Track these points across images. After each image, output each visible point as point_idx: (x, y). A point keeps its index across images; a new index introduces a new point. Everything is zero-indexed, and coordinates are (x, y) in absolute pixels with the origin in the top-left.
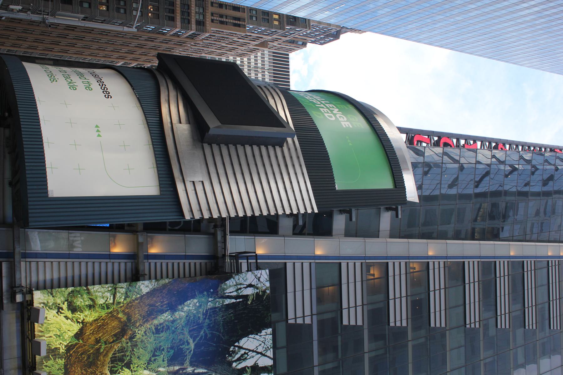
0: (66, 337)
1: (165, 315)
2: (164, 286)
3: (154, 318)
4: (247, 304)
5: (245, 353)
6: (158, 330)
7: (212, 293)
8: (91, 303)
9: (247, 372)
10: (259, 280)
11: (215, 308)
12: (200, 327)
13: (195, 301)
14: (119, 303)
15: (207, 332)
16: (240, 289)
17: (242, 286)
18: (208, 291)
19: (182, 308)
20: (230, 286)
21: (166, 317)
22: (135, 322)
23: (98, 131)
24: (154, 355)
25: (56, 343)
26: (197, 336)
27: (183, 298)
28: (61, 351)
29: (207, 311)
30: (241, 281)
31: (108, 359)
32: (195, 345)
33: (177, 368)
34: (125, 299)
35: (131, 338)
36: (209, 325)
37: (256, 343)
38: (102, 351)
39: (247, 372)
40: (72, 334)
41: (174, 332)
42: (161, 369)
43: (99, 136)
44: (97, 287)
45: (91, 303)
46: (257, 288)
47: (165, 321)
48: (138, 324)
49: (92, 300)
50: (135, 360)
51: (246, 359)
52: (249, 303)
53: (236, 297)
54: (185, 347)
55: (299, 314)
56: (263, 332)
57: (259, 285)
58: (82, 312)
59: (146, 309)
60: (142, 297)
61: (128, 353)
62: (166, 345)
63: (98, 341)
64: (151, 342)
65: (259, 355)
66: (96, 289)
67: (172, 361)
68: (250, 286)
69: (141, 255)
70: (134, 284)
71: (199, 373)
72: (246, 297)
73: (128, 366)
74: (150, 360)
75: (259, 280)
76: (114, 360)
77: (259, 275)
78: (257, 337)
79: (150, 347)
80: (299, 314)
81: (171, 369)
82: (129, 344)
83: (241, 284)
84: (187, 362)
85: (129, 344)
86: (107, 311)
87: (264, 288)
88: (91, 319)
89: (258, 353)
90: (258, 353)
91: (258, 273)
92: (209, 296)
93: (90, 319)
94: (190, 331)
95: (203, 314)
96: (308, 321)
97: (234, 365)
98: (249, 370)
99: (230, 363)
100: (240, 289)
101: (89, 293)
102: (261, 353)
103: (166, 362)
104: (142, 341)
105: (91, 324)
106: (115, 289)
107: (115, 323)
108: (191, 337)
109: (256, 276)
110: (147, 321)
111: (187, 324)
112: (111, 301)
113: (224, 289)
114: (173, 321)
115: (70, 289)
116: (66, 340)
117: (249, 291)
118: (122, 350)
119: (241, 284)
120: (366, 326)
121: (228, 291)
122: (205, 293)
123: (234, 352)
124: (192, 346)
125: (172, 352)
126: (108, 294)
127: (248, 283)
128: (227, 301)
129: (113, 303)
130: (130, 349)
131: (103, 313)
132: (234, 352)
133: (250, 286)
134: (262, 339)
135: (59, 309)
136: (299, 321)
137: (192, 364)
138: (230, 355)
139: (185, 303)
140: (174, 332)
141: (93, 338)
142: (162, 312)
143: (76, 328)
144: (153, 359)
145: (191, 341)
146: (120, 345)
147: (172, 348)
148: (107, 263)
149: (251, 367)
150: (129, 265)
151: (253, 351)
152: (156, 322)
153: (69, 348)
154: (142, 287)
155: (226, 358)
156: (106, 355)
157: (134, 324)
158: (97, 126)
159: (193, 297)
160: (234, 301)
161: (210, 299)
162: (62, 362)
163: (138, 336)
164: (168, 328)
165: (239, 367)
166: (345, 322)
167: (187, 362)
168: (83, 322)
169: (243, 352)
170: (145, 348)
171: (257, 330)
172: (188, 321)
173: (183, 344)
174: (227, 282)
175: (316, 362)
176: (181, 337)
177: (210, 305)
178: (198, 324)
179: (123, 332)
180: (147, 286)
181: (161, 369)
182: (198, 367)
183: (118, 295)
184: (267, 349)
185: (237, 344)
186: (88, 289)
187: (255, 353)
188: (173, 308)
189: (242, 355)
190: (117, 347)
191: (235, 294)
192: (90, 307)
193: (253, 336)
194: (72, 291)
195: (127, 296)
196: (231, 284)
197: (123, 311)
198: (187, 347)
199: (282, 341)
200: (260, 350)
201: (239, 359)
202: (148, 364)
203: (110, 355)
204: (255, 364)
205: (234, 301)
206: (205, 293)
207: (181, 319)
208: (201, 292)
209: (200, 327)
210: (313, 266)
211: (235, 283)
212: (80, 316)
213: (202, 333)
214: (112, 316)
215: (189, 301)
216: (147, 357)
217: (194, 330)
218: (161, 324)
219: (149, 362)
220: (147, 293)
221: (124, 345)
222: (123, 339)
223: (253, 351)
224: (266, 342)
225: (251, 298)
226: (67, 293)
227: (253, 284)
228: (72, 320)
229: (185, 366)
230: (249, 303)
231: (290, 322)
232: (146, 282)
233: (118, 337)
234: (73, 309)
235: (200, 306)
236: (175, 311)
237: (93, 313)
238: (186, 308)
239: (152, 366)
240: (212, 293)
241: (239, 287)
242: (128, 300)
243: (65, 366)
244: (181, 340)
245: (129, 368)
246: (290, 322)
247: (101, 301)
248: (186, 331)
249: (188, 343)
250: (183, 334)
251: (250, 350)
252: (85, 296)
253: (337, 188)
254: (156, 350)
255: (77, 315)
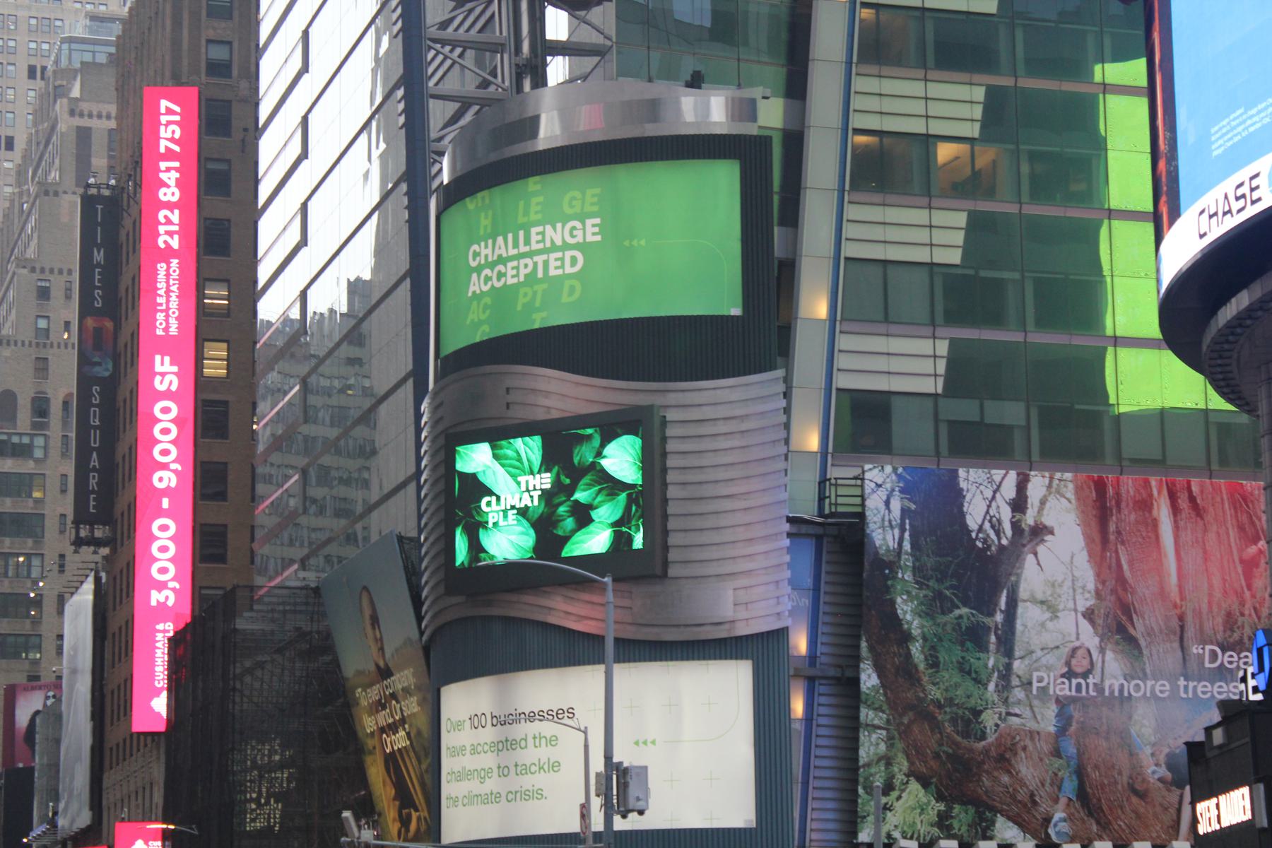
0: (924, 800)
1: (913, 650)
2: (871, 648)
3: (917, 670)
4: (914, 512)
5: (990, 521)
6: (934, 664)
7: (891, 571)
8: (883, 762)
9: (1019, 521)
10: (880, 486)
11: (914, 567)
12: (939, 595)
13: (899, 600)
14: (888, 721)
15: (948, 584)
16: (890, 521)
17: (887, 518)
18: (887, 578)
19: (908, 622)
20: (884, 539)
21: (916, 650)
22: (919, 699)
23: (645, 743)
24: (969, 673)
25: (932, 815)
26: (952, 601)
27: (893, 620)
28: (942, 808)
29: (917, 583)
30: (877, 519)
31: (965, 742)
32: (965, 605)
33: (993, 638)
34: (883, 712)
35: (939, 706)
36: (937, 580)
37: (979, 497)
38: (950, 751)
39: (1019, 521)
40: (922, 792)
41: (940, 640)
42: (991, 663)
43: (653, 742)
44: (862, 753)
45: (883, 762)
46: (893, 490)
47: (922, 652)
48: (922, 695)
49: (879, 760)
50: (972, 702)
51: (999, 521)
52: (913, 507)
53: (903, 530)
54: (965, 623)
55: (927, 366)
56: (963, 485)
57: (888, 486)
58: (893, 777)
59: (901, 680)
60: (883, 685)
61: (960, 712)
62: (958, 652)
63: (937, 756)
64: (949, 676)
65: (998, 495)
66: (864, 754)
67: (982, 647)
68: (887, 503)
69: (812, 672)
70: (863, 697)
71: (1007, 603)
72: (905, 512)
73: (977, 713)
74: (975, 680)
75: (880, 486)
76: (966, 734)
77: (873, 485)
78: (968, 497)
79: (957, 678)
80: (927, 366)
81: (992, 647)
82: (948, 710)
83: (883, 520)
84: (987, 620)
85: (948, 710)
86: (897, 741)
87: (894, 477)
88: (906, 763)
89: (994, 497)
90: (994, 497)
91: (869, 486)
92: (895, 578)
93: (905, 765)
94: (943, 613)
95: (920, 589)
96: (943, 348)
97: (1004, 542)
98: (1018, 516)
99: (1001, 548)
100: (890, 521)
101: (868, 765)
102: (995, 492)
103: (982, 655)
104: (946, 690)
105: (912, 763)
106: (867, 725)
107: (916, 729)
108: (951, 612)
109: (873, 491)
110: (919, 680)
111: (933, 618)
112: (884, 732)
113: (888, 550)
114: (925, 639)
115: (861, 791)
116: (929, 802)
117: (896, 505)
118: (954, 721)
119: (883, 520)
120: (970, 204)
121: (891, 544)
122: (889, 583)
123: (985, 541)
124: (964, 611)
125: (969, 644)
126: (874, 736)
127: (882, 506)
128: (907, 546)
129: (887, 729)
130: (955, 709)
131: (899, 745)
132: (985, 541)
133: (887, 503)
134: (974, 488)
135: (887, 808)
136: (941, 367)
137: (991, 614)
138: (989, 547)
139: (901, 617)
140: (940, 640)
141: (932, 763)
142: (909, 655)
143: (914, 786)
144: (974, 675)
145: (957, 612)
146: (946, 724)
147: (962, 644)
148: (818, 726)
149: (1013, 511)
150: (823, 689)
151: (989, 506)
152: (922, 667)
153: (940, 798)
154: (869, 684)
155: (992, 556)
156: (957, 744)
157: (920, 700)
158: (637, 743)
159: (893, 602)
160: (907, 535)
161: (900, 575)
162: (957, 809)
163: (938, 696)
164: (933, 648)
165: (1009, 532)
166: (955, 257)
167: (987, 620)
168: (907, 776)
169: (987, 525)
170: (957, 686)
171: (958, 495)
172: (927, 614)
173: (959, 625)
174: (878, 543)
175: (1017, 337)
176: (949, 628)
177: (908, 576)
178: (934, 599)
179: (930, 718)
180: (869, 676)
181: (991, 663)
182: (996, 604)
183: (876, 722)
184: (991, 481)
185: (974, 535)
186: (864, 766)
187: (994, 504)
188: (905, 638)
189: (993, 527)
190: (949, 729)
191: (897, 532)
192: (889, 764)
193: (966, 505)
194: (865, 788)
195: (880, 709)
196: (880, 537)
197: (901, 715)
198: (965, 620)
199: (874, 69)
200: (989, 494)
201: (998, 533)
202: (979, 682)
203: (959, 739)
204: (1009, 504)
205: (907, 535)
206: (889, 583)
207: (922, 627)
208: (887, 589)
209: (939, 595)
210: (847, 327)
211: (880, 531)
212: (900, 777)
213: (948, 593)
214: (905, 733)
215: (899, 611)
216: (969, 684)
217: (942, 607)
218: (926, 659)
219: (977, 681)
220: (879, 677)
221: (948, 717)
222: (940, 718)
223: (989, 506)
224: (979, 481)
225: (907, 503)
226: (866, 796)
227: (884, 498)
228: (903, 791)
229: (992, 625)
230: (913, 507)
231: (940, 391)
232: (863, 677)
233: (936, 726)
234: (888, 788)
235: (908, 593)
236: (910, 634)
237: (898, 760)
238: (908, 617)
239: (984, 677)
240: (891, 571)
241: (887, 523)
242: (885, 707)
243: (963, 803)
244: (954, 629)
245: (981, 712)
246: (940, 391)
247: (883, 747)
248: (942, 619)
249: (961, 617)
250: (945, 624)
251: (987, 512)
252: (873, 770)
253: (736, 311)
254: (962, 670)
255: (897, 782)
